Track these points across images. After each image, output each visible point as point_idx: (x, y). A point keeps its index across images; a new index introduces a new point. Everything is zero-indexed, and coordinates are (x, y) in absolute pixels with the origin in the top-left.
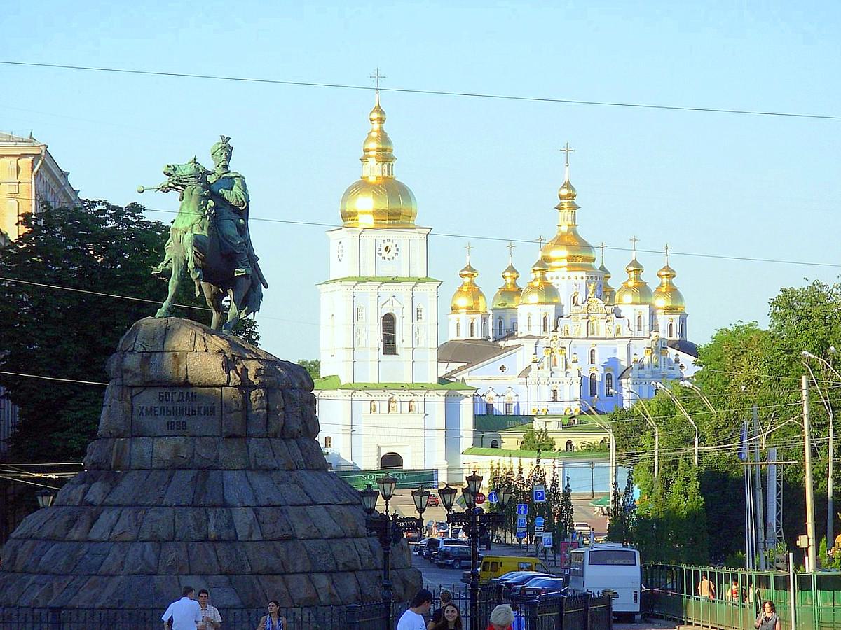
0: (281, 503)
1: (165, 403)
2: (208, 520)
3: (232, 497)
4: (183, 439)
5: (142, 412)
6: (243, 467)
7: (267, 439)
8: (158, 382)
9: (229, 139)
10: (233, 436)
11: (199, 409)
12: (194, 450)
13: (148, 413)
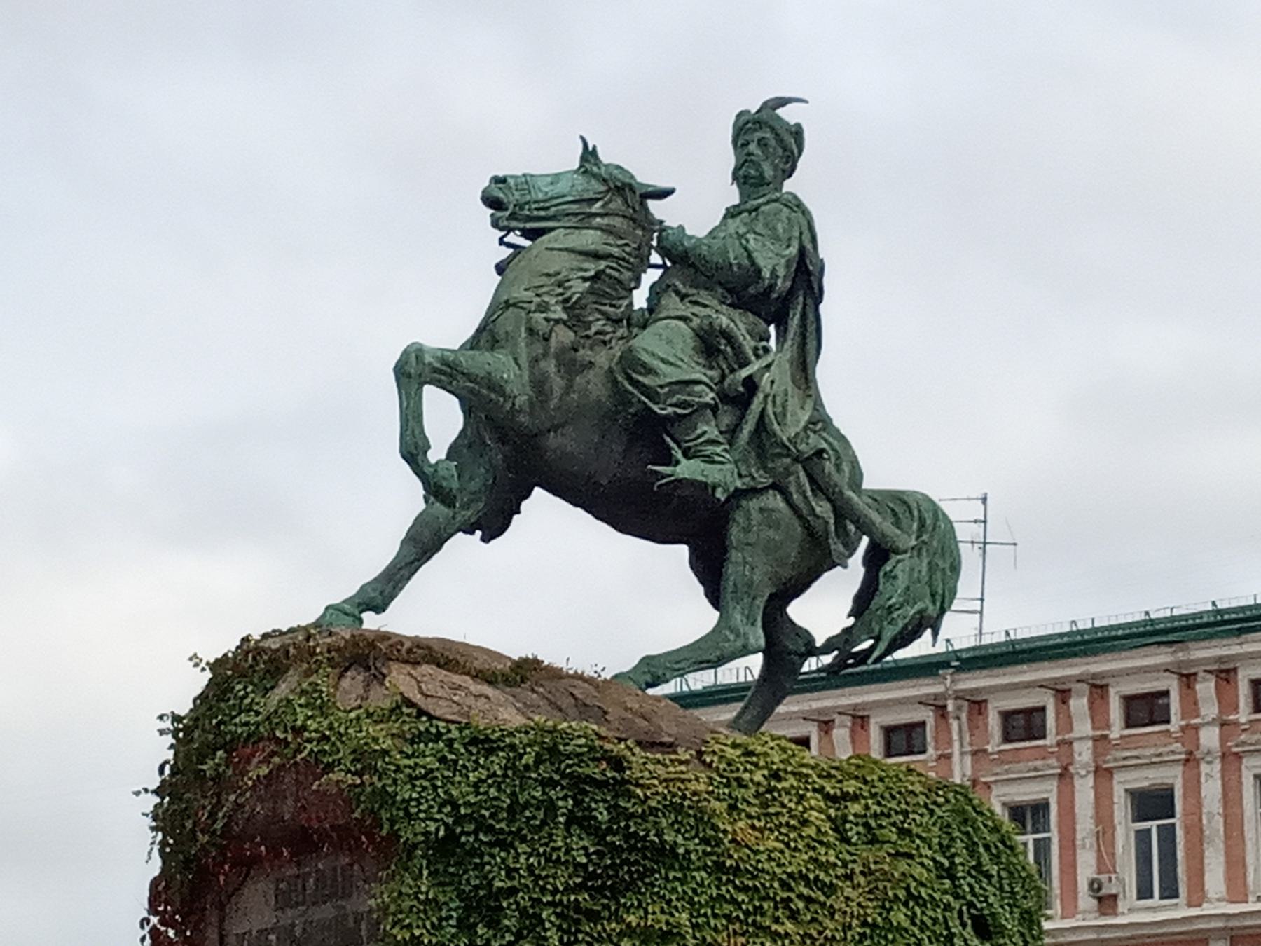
9: (783, 102)
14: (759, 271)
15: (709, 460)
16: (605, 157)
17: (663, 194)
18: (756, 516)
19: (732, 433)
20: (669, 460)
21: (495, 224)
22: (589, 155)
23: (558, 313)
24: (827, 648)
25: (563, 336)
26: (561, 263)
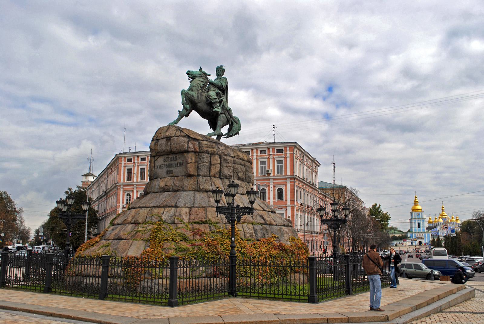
0: (206, 206)
1: (166, 163)
2: (163, 213)
3: (181, 203)
4: (170, 178)
5: (157, 168)
6: (193, 190)
7: (209, 178)
8: (161, 152)
9: (223, 66)
10: (190, 176)
11: (178, 164)
12: (174, 182)
13: (160, 168)
14: (223, 86)
15: (218, 109)
16: (203, 70)
17: (209, 75)
18: (222, 117)
19: (220, 105)
20: (213, 108)
21: (188, 77)
22: (200, 69)
23: (200, 88)
24: (225, 135)
25: (200, 91)
26: (199, 82)
